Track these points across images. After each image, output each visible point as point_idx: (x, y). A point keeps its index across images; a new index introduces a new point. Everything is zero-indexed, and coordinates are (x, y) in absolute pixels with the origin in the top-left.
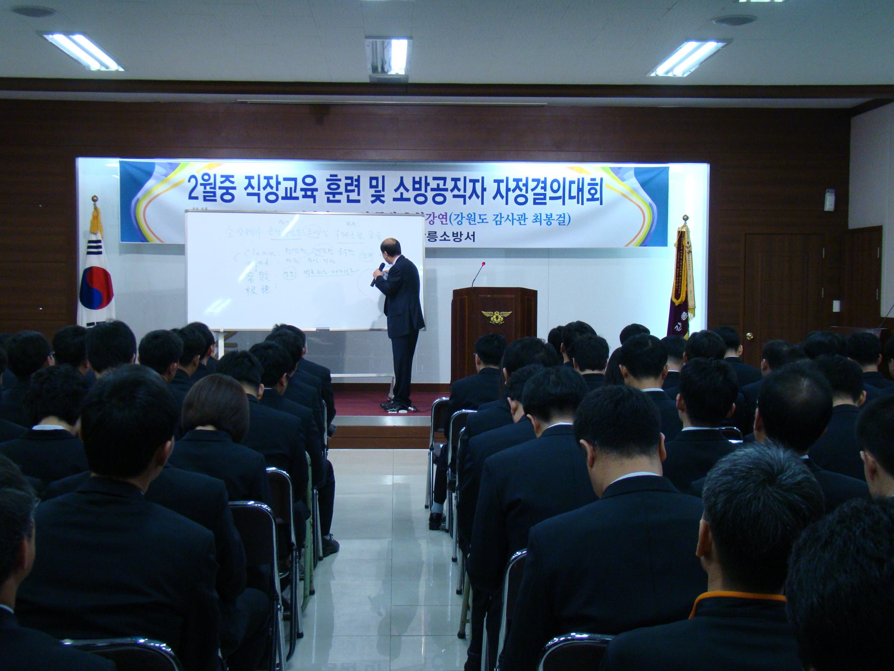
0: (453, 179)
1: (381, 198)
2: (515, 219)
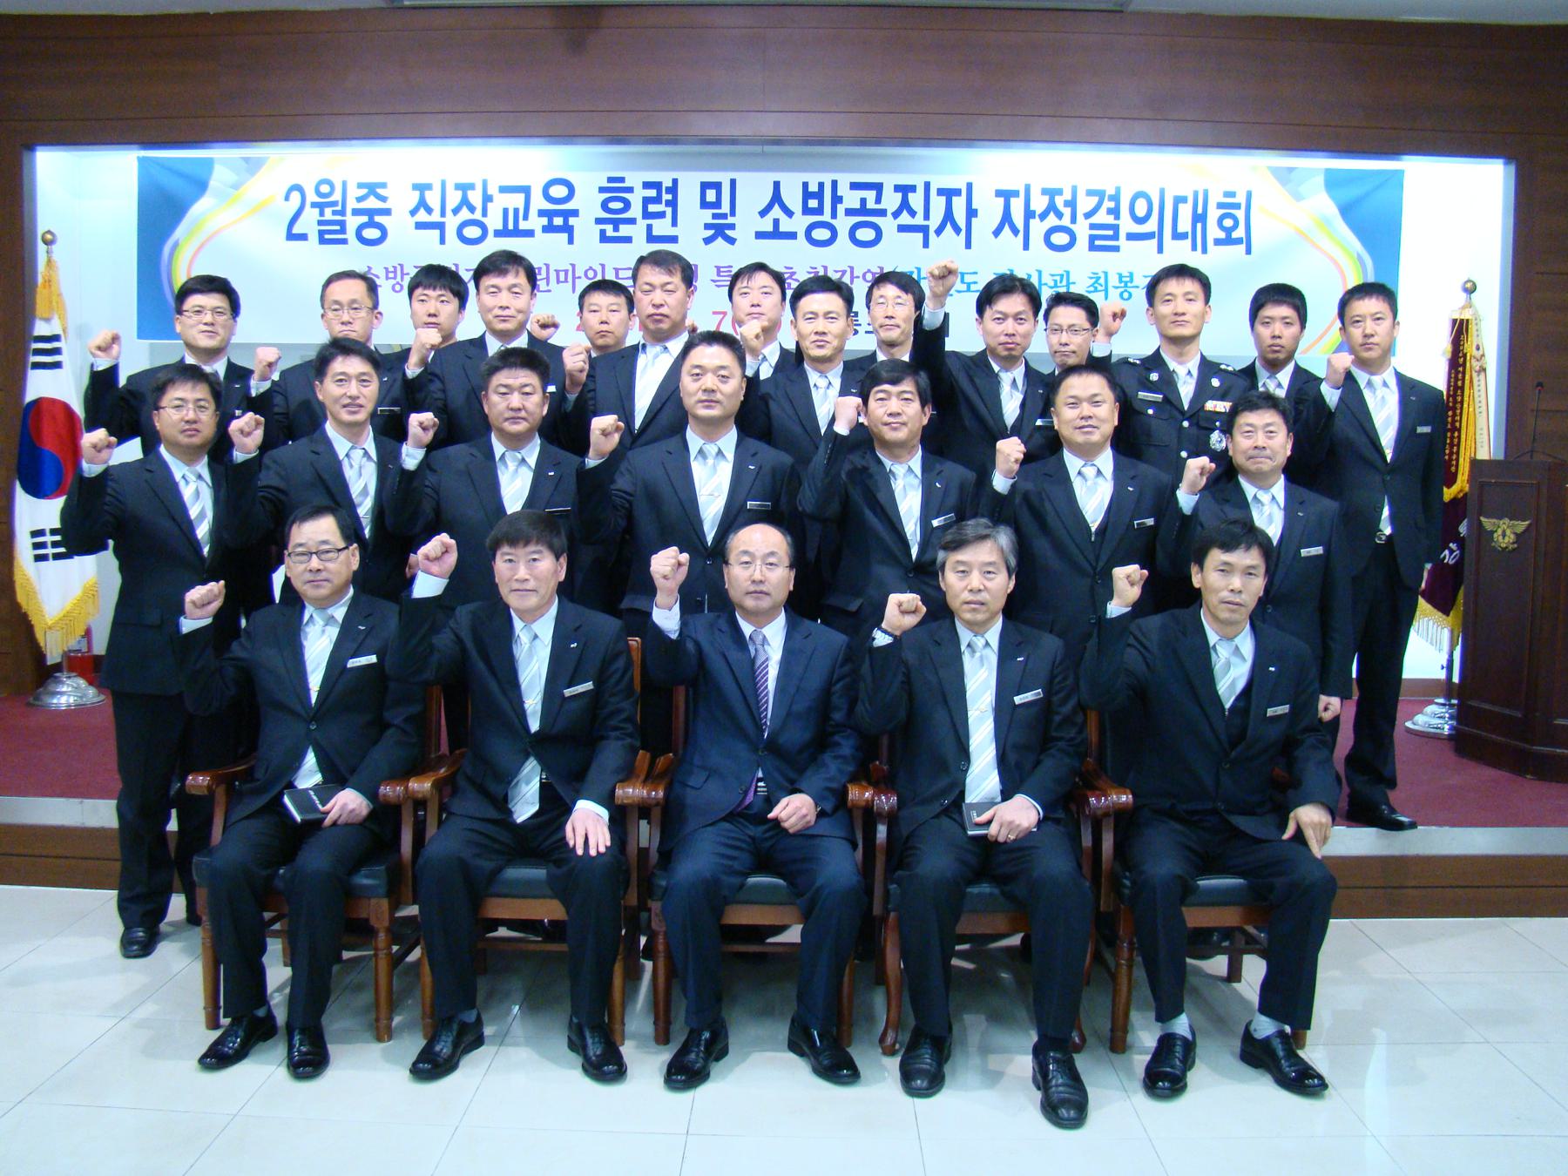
0: (898, 188)
1: (728, 232)
2: (1045, 284)
